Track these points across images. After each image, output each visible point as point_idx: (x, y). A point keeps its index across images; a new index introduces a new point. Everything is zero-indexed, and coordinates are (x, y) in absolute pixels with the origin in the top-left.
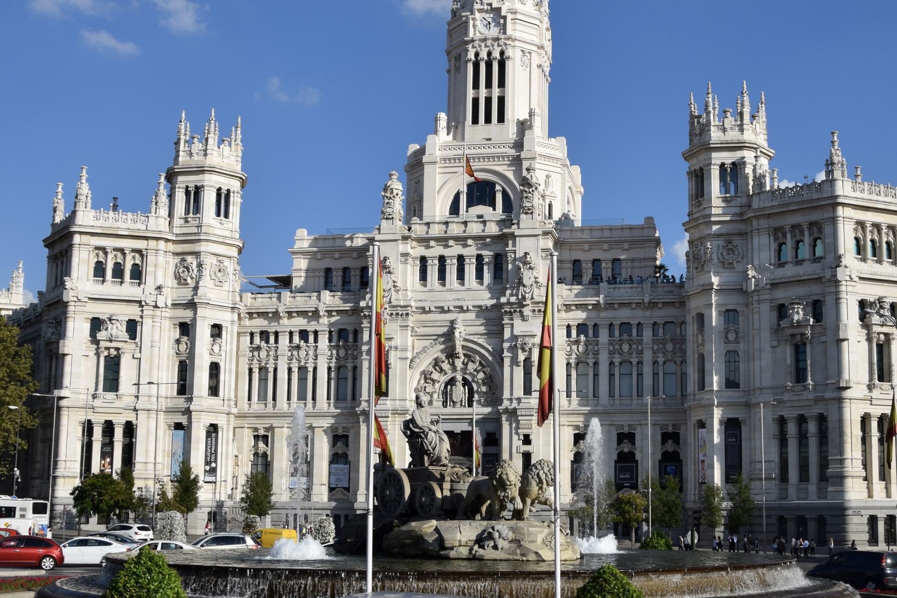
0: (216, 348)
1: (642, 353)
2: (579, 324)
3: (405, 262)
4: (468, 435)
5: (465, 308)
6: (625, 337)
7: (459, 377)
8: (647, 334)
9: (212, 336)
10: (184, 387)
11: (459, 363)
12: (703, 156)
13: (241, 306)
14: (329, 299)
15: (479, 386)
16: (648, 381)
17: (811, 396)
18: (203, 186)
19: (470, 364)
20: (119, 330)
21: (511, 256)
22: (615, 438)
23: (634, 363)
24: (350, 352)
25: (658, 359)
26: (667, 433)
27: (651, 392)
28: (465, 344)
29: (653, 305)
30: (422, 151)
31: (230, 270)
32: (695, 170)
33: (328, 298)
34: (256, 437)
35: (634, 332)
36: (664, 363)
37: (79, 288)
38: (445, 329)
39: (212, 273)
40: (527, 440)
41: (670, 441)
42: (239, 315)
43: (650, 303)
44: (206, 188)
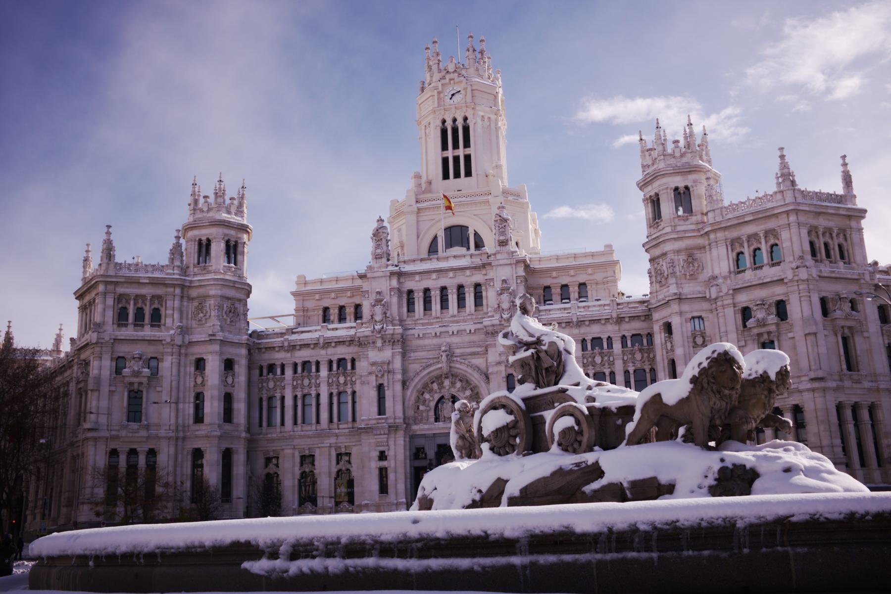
0: (230, 380)
1: (614, 364)
6: (597, 350)
7: (447, 396)
8: (617, 346)
9: (225, 370)
11: (447, 383)
23: (607, 373)
25: (629, 369)
28: (452, 365)
29: (620, 320)
32: (651, 197)
39: (224, 313)
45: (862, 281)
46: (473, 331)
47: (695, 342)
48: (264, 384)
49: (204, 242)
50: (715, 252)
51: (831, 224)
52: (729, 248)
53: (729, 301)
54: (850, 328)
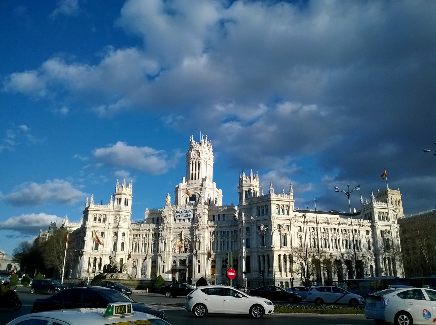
0: (123, 239)
2: (213, 232)
3: (170, 216)
4: (185, 261)
5: (185, 228)
7: (183, 246)
8: (230, 234)
9: (122, 235)
10: (115, 249)
11: (183, 242)
12: (241, 188)
13: (130, 228)
14: (153, 226)
15: (188, 248)
16: (230, 246)
17: (265, 250)
18: (121, 198)
19: (186, 242)
20: (99, 235)
21: (196, 214)
22: (222, 261)
24: (157, 239)
26: (235, 260)
27: (231, 249)
28: (185, 237)
30: (178, 187)
31: (128, 219)
33: (152, 225)
34: (134, 262)
35: (227, 233)
36: (234, 241)
37: (90, 224)
38: (180, 233)
40: (199, 262)
41: (235, 262)
42: (130, 230)
43: (230, 226)
44: (122, 199)
45: (291, 220)
46: (191, 227)
47: (247, 235)
48: (134, 240)
49: (119, 199)
50: (253, 210)
51: (283, 204)
52: (257, 209)
53: (255, 224)
54: (285, 233)
